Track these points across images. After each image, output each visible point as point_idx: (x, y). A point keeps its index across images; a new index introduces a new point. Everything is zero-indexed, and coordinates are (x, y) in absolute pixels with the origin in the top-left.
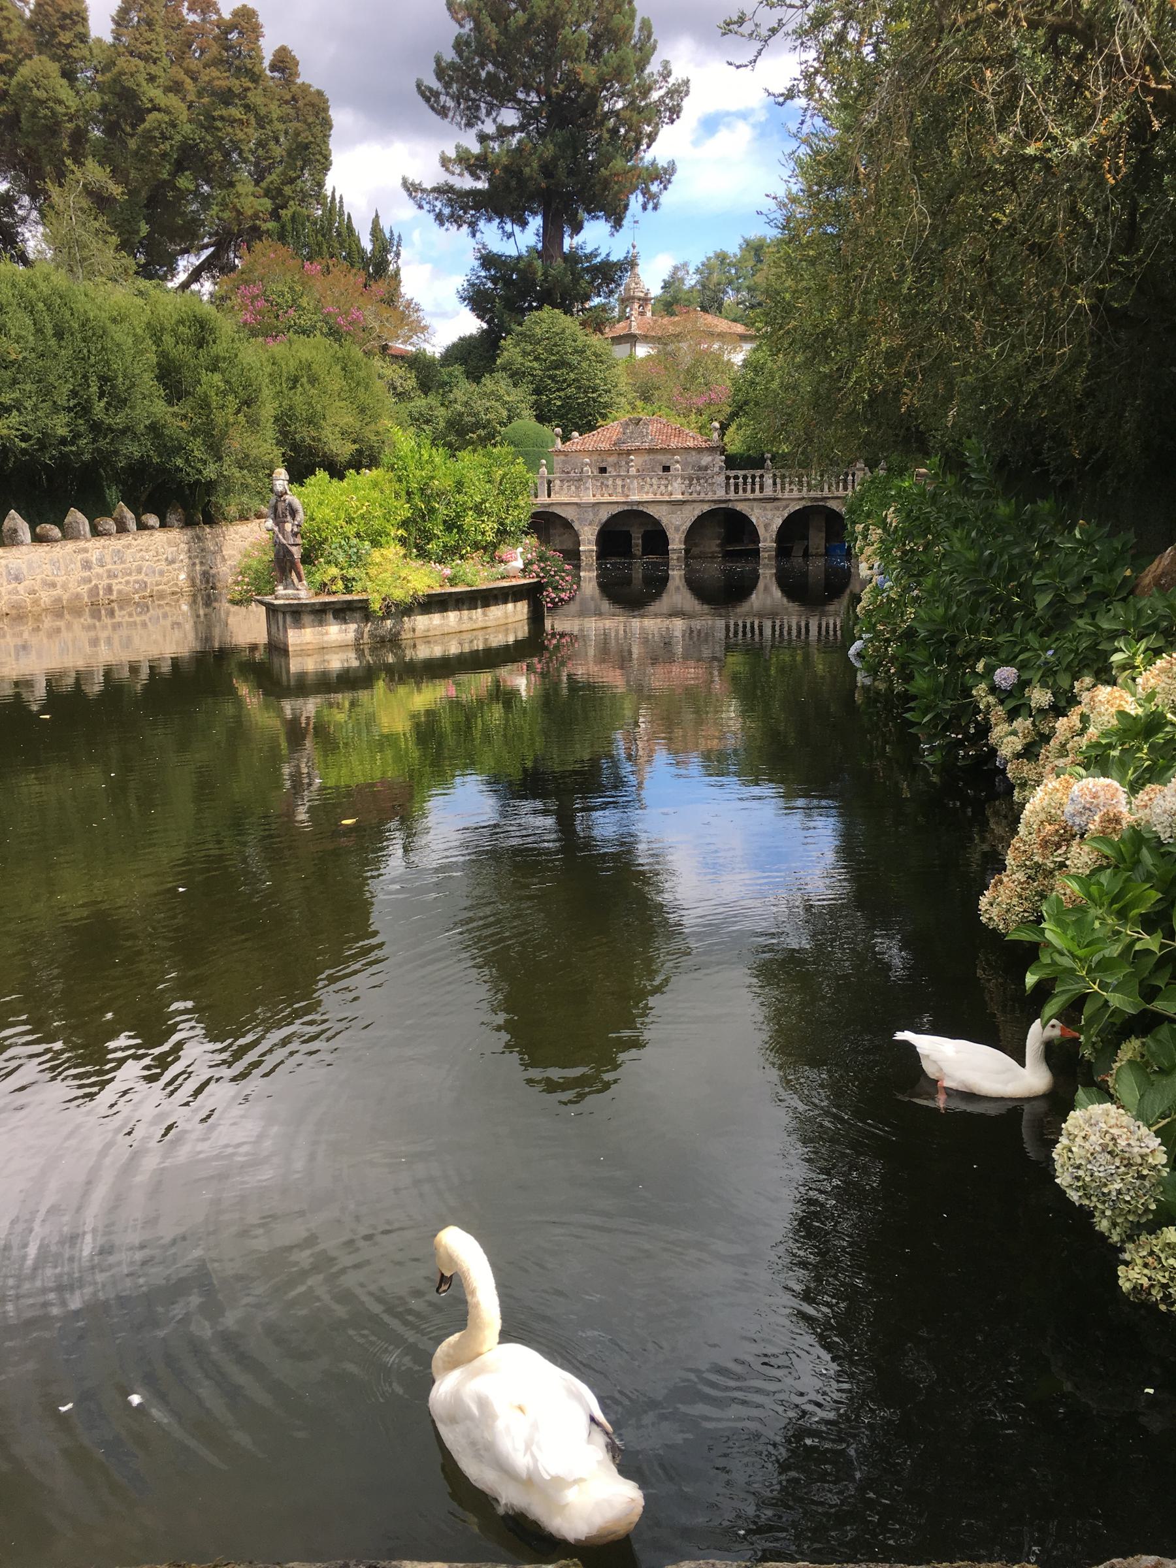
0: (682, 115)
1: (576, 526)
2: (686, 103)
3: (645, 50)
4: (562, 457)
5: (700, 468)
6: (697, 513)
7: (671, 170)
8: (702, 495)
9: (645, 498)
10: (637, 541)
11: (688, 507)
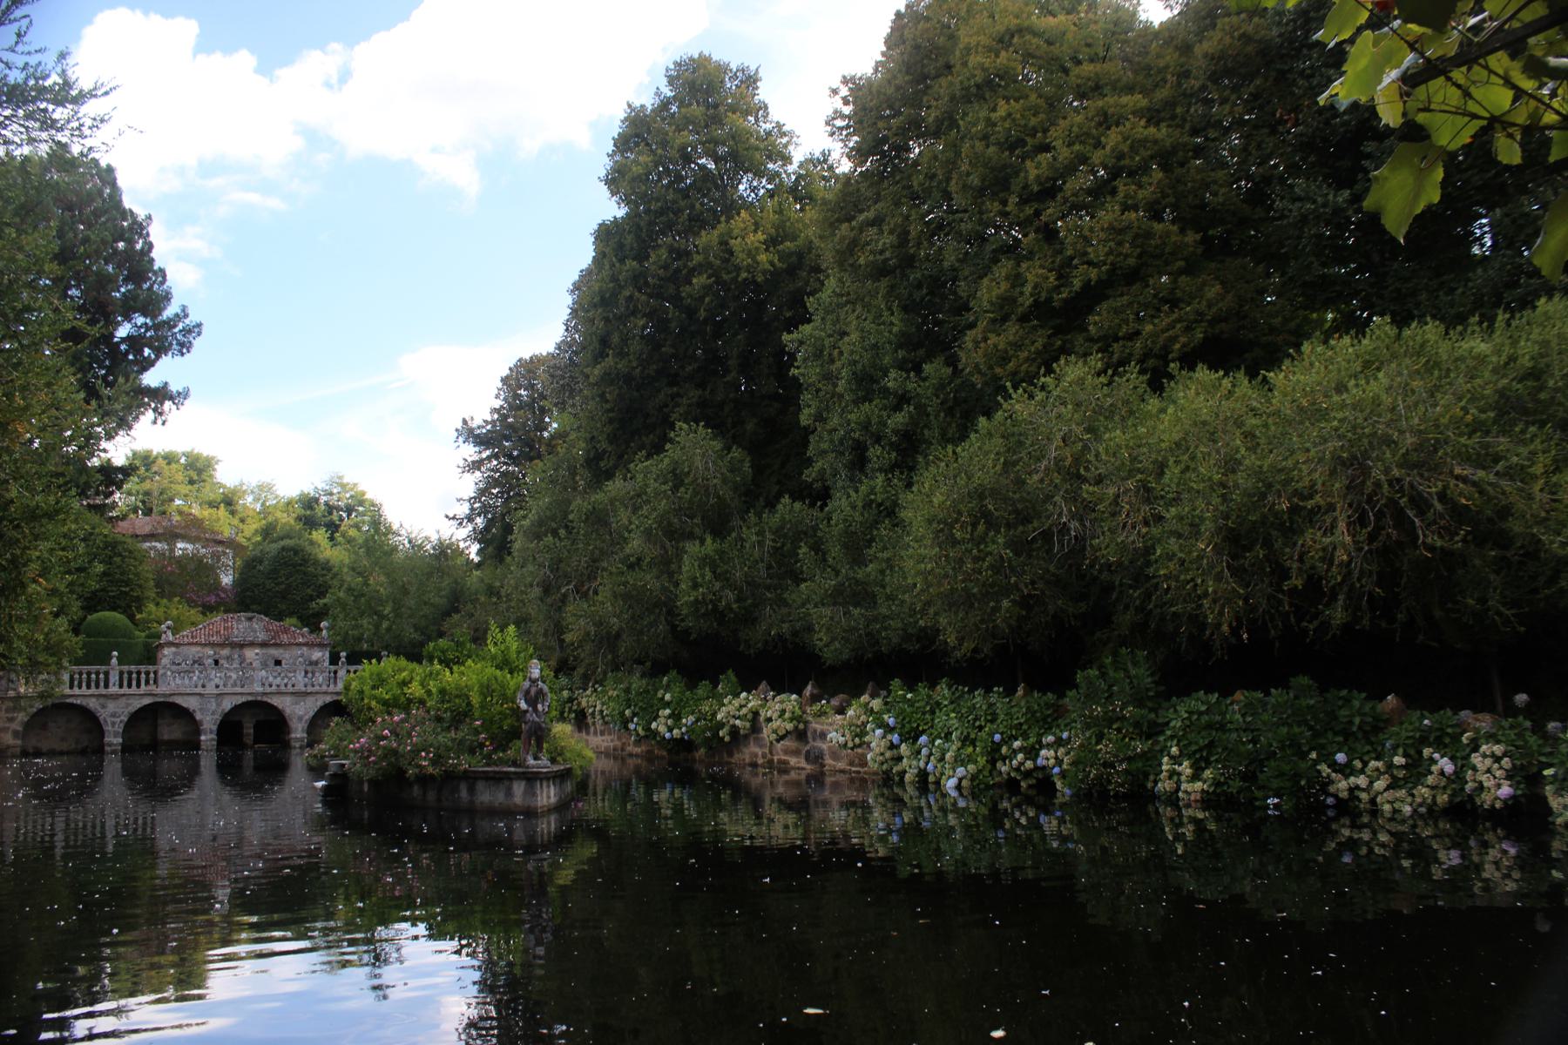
0: (193, 350)
1: (198, 716)
2: (198, 343)
3: (167, 297)
4: (173, 649)
5: (311, 663)
6: (320, 703)
7: (184, 394)
8: (324, 688)
9: (268, 690)
10: (249, 730)
11: (310, 699)
